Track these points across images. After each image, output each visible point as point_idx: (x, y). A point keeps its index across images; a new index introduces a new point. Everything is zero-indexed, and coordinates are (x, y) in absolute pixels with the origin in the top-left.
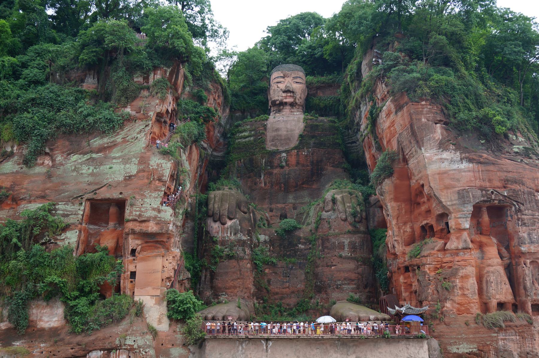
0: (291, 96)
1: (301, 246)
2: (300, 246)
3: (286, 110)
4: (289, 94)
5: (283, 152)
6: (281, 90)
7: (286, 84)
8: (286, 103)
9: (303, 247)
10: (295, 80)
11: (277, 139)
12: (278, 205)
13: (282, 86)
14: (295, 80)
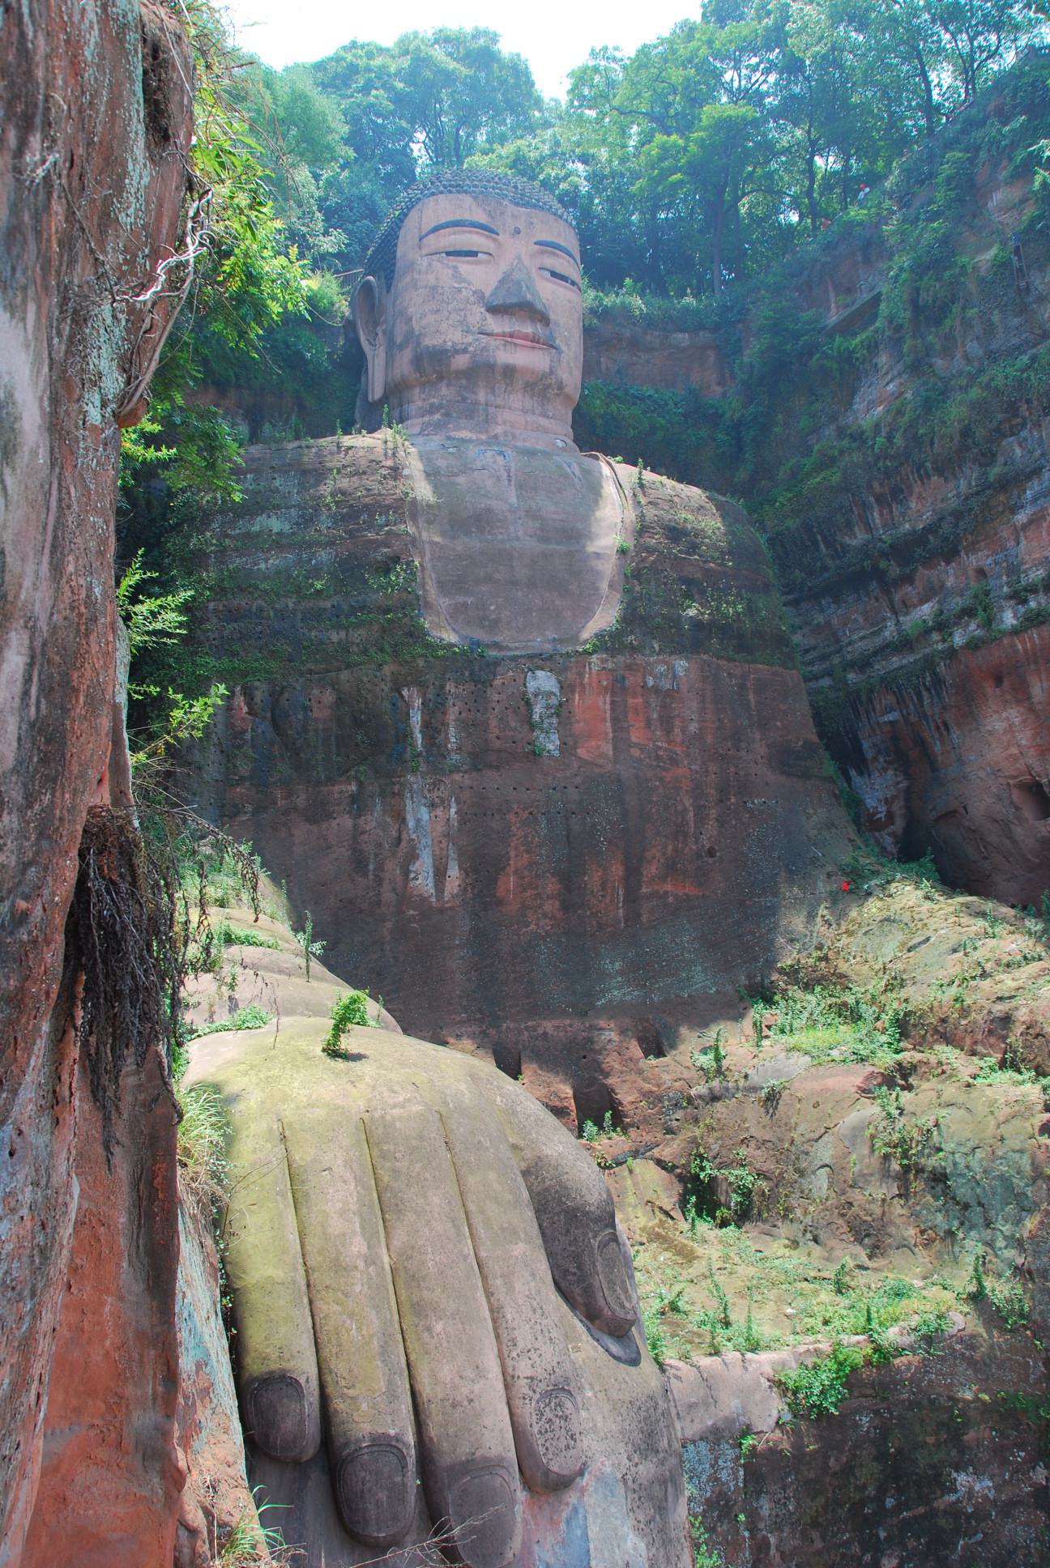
0: (535, 339)
1: (971, 1485)
2: (962, 1479)
3: (507, 415)
4: (528, 329)
5: (540, 660)
6: (480, 296)
7: (504, 267)
8: (509, 372)
9: (984, 1486)
10: (549, 262)
11: (488, 579)
12: (548, 1026)
13: (482, 277)
14: (549, 262)
